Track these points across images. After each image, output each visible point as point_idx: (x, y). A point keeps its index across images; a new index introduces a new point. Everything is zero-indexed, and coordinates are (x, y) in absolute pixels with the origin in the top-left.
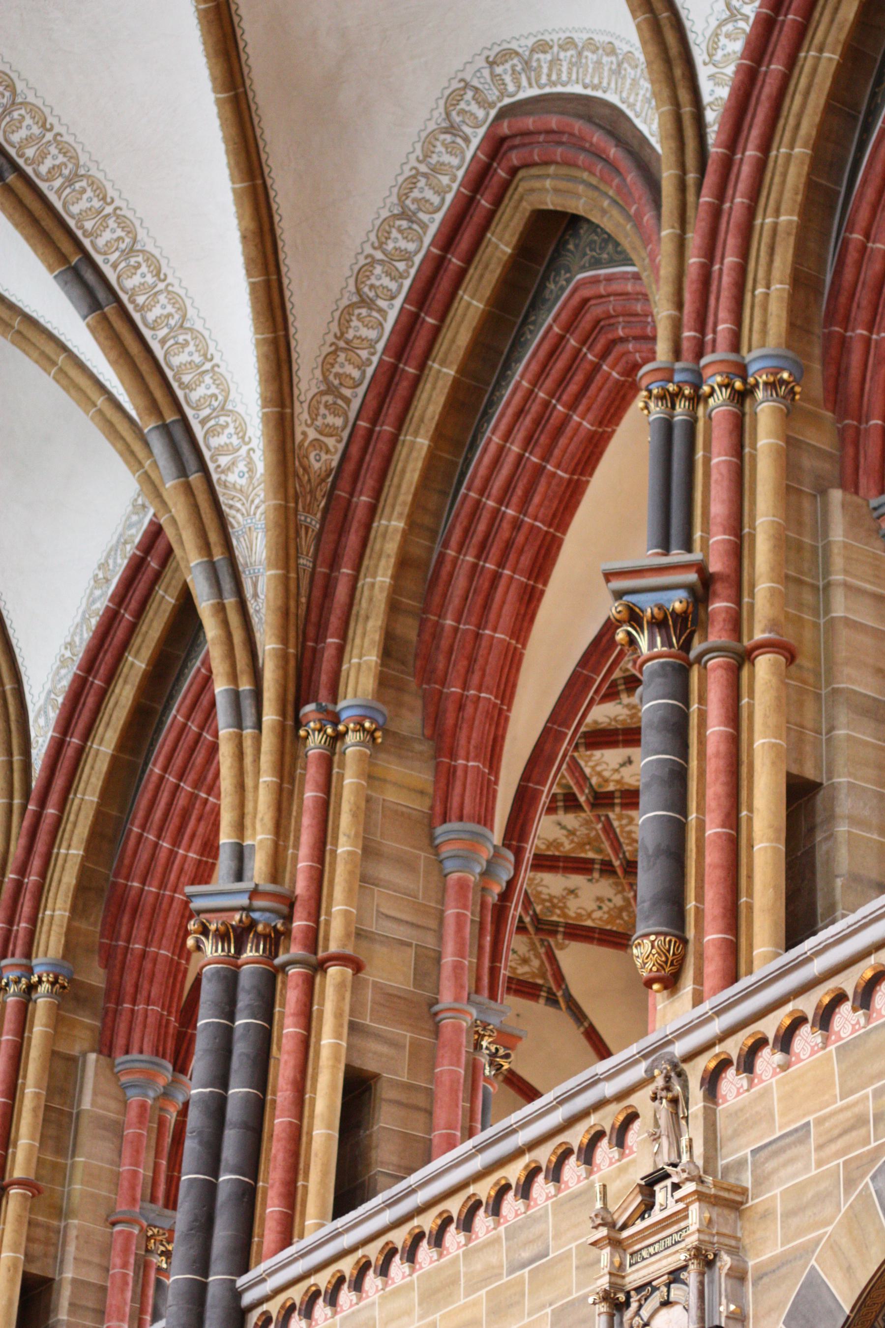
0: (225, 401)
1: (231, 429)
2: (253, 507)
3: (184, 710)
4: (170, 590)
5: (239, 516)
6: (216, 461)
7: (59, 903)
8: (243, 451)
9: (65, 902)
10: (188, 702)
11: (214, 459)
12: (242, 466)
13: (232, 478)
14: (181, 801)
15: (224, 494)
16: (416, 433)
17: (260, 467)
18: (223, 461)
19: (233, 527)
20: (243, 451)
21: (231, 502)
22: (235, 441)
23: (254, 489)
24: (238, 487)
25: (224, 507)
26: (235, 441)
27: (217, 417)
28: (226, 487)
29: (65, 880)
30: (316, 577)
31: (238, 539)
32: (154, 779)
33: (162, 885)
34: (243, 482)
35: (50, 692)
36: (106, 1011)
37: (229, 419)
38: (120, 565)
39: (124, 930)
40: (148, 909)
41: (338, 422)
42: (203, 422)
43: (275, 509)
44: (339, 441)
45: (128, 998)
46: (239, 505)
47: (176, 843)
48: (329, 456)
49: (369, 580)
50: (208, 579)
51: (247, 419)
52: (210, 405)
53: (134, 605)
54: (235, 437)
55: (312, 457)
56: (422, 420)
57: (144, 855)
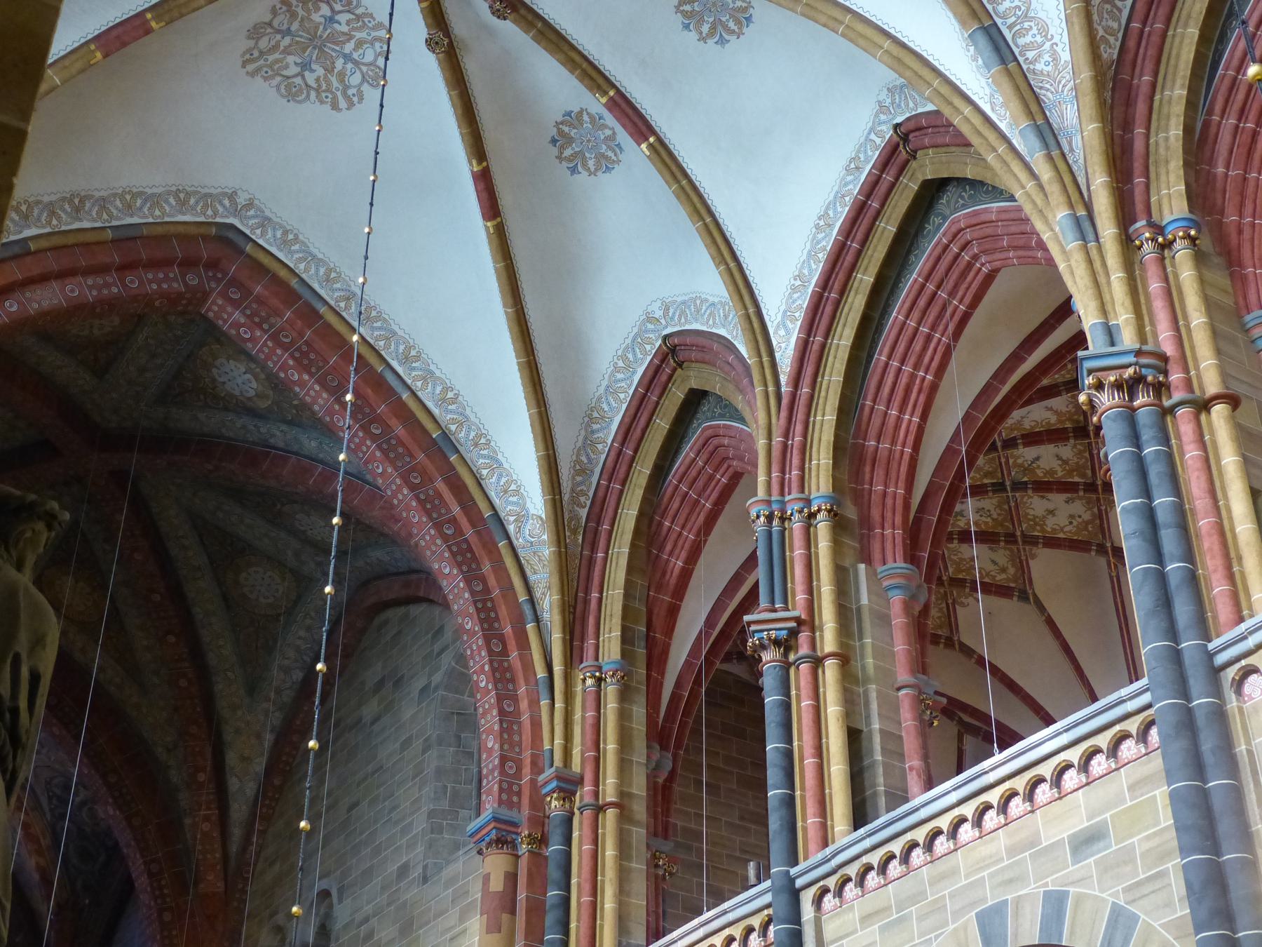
0: (1028, 11)
1: (1035, 31)
2: (1061, 86)
3: (904, 311)
4: (892, 221)
5: (1049, 94)
6: (1025, 55)
7: (822, 455)
8: (1047, 45)
9: (828, 453)
10: (907, 305)
11: (1022, 54)
12: (1047, 57)
13: (1039, 66)
14: (904, 380)
15: (1034, 79)
16: (1186, 26)
17: (1065, 56)
18: (1030, 55)
19: (1045, 103)
20: (1047, 45)
21: (1040, 84)
22: (1039, 39)
23: (1059, 73)
24: (1046, 73)
25: (1035, 89)
26: (1039, 39)
27: (1022, 23)
28: (1035, 73)
29: (824, 438)
30: (1115, 138)
31: (1050, 111)
32: (881, 364)
33: (893, 442)
34: (1049, 68)
35: (785, 312)
36: (862, 536)
37: (1032, 24)
38: (842, 213)
39: (867, 477)
40: (884, 461)
41: (1115, 25)
42: (1010, 27)
43: (1091, 78)
44: (1117, 40)
45: (878, 525)
46: (1048, 86)
47: (902, 410)
48: (1111, 51)
49: (1162, 135)
50: (1037, 136)
51: (1049, 22)
52: (1015, 14)
53: (860, 236)
54: (1039, 36)
55: (1102, 48)
56: (1189, 16)
57: (876, 421)
